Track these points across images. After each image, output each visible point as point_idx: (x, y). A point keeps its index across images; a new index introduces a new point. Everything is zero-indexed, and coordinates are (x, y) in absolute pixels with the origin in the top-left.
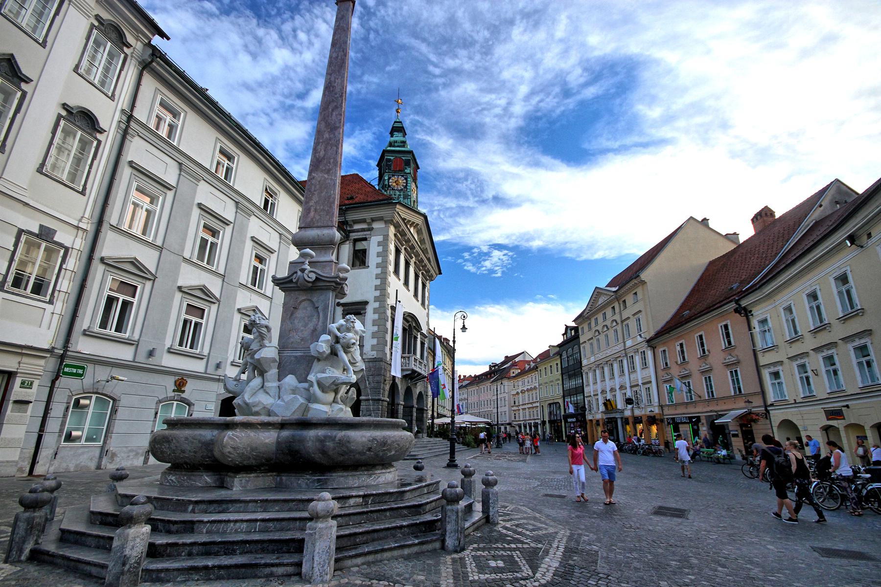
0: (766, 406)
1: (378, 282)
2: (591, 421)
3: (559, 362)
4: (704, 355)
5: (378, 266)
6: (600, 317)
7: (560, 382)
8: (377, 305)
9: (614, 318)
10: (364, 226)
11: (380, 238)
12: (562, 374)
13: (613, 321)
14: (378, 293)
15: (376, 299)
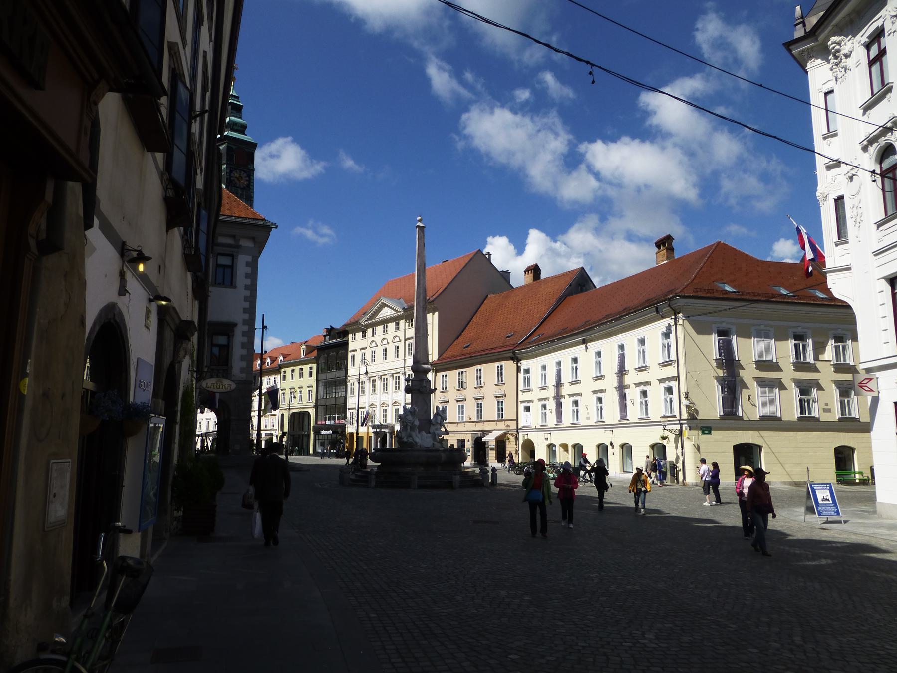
0: (517, 429)
1: (247, 305)
2: (351, 434)
3: (315, 366)
4: (479, 386)
5: (246, 287)
6: (380, 329)
7: (314, 390)
8: (246, 328)
9: (397, 333)
10: (230, 241)
11: (249, 258)
12: (318, 380)
13: (396, 336)
14: (246, 316)
15: (245, 322)
